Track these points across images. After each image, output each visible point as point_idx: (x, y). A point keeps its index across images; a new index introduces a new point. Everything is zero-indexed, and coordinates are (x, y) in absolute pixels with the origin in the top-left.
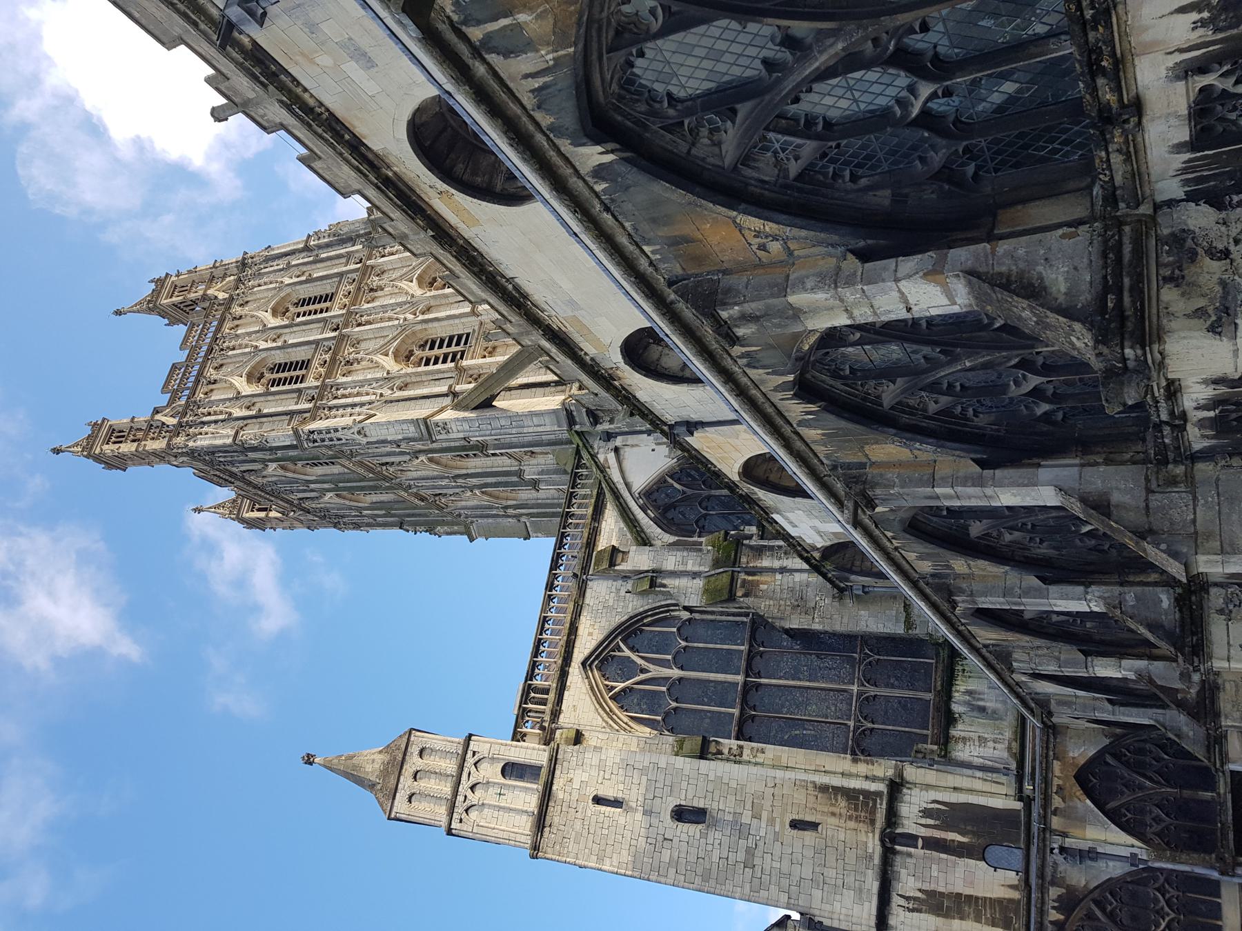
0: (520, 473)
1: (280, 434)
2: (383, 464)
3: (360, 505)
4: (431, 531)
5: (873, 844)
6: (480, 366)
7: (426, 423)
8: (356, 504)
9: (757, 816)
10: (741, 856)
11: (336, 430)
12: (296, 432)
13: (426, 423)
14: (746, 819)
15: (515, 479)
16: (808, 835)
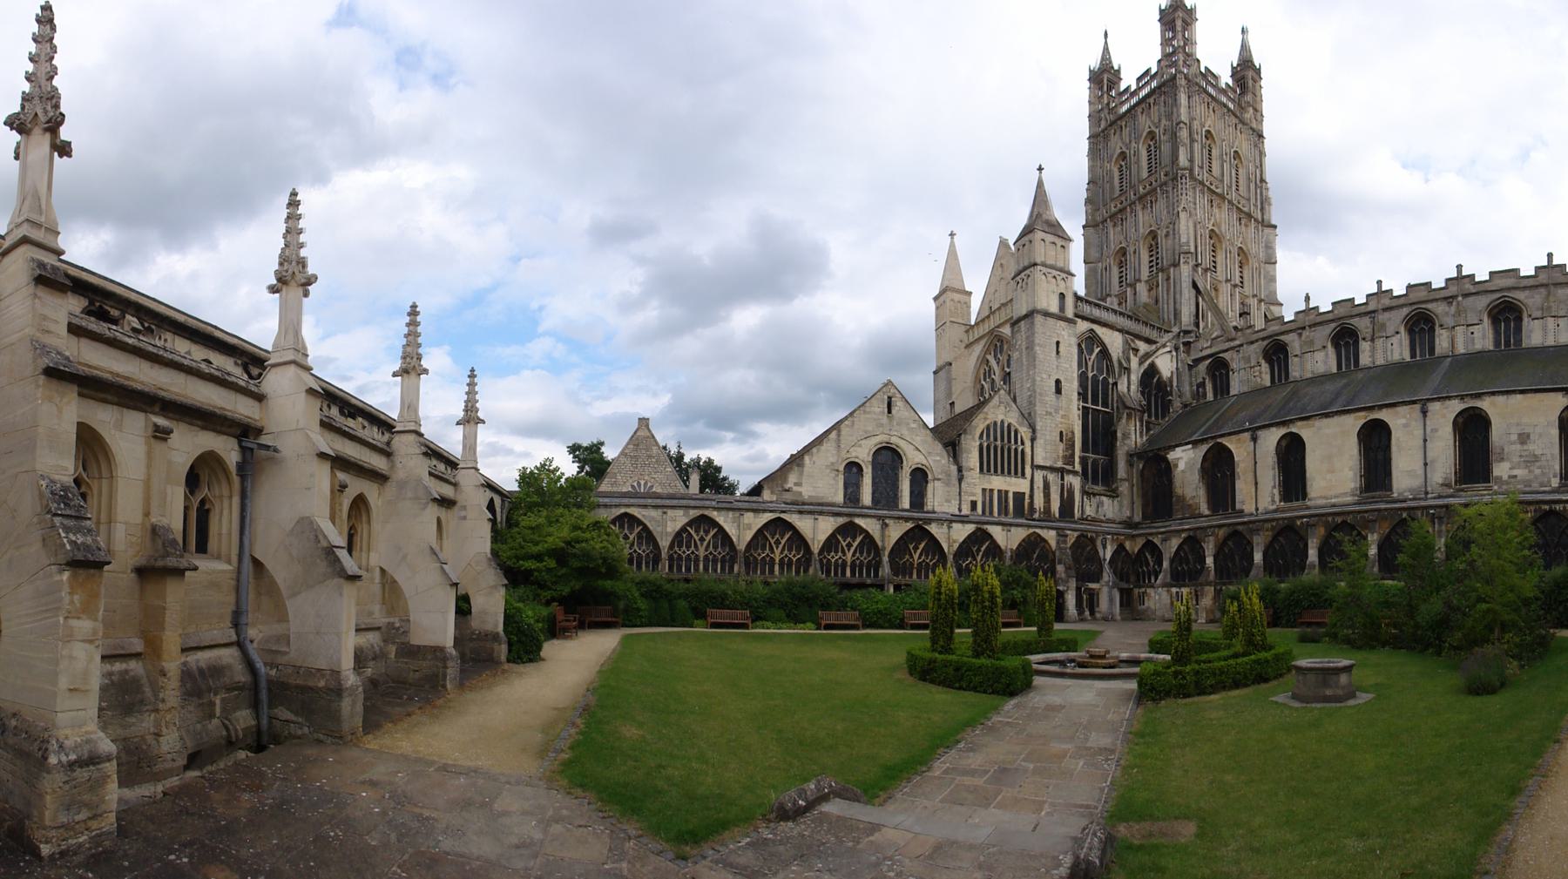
0: (1139, 280)
1: (1183, 160)
2: (1152, 202)
3: (1113, 164)
4: (1088, 201)
5: (1059, 464)
6: (1206, 281)
7: (1189, 253)
8: (1114, 160)
9: (1063, 417)
10: (1049, 410)
11: (1187, 194)
12: (1185, 169)
13: (1189, 253)
14: (1061, 412)
15: (1137, 277)
16: (1058, 438)
